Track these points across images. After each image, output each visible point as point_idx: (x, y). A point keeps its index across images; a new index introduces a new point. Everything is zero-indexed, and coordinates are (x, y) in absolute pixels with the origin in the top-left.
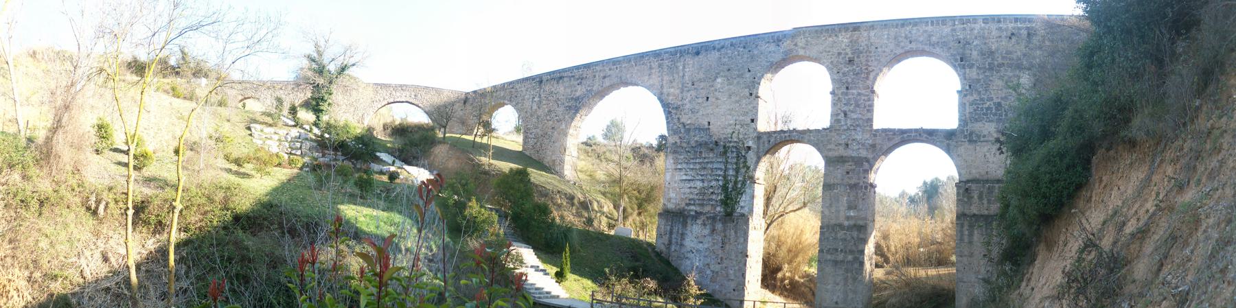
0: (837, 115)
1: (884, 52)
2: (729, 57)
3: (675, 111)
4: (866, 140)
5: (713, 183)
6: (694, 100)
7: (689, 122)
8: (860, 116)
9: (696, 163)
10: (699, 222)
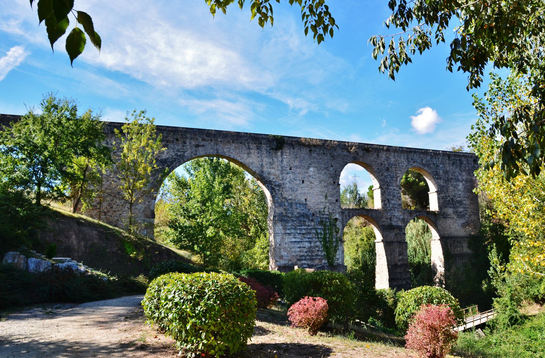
0: (385, 201)
1: (403, 166)
2: (317, 154)
3: (278, 188)
4: (400, 216)
5: (318, 244)
6: (293, 182)
7: (290, 198)
9: (302, 229)
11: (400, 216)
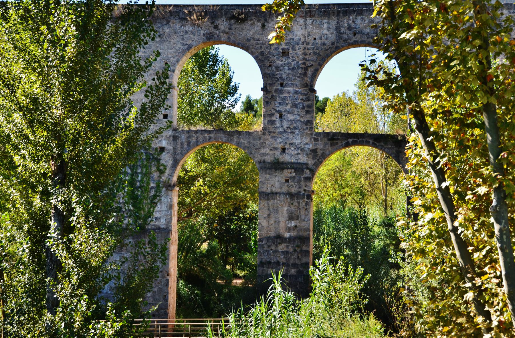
4: (307, 144)
8: (298, 118)
11: (307, 144)
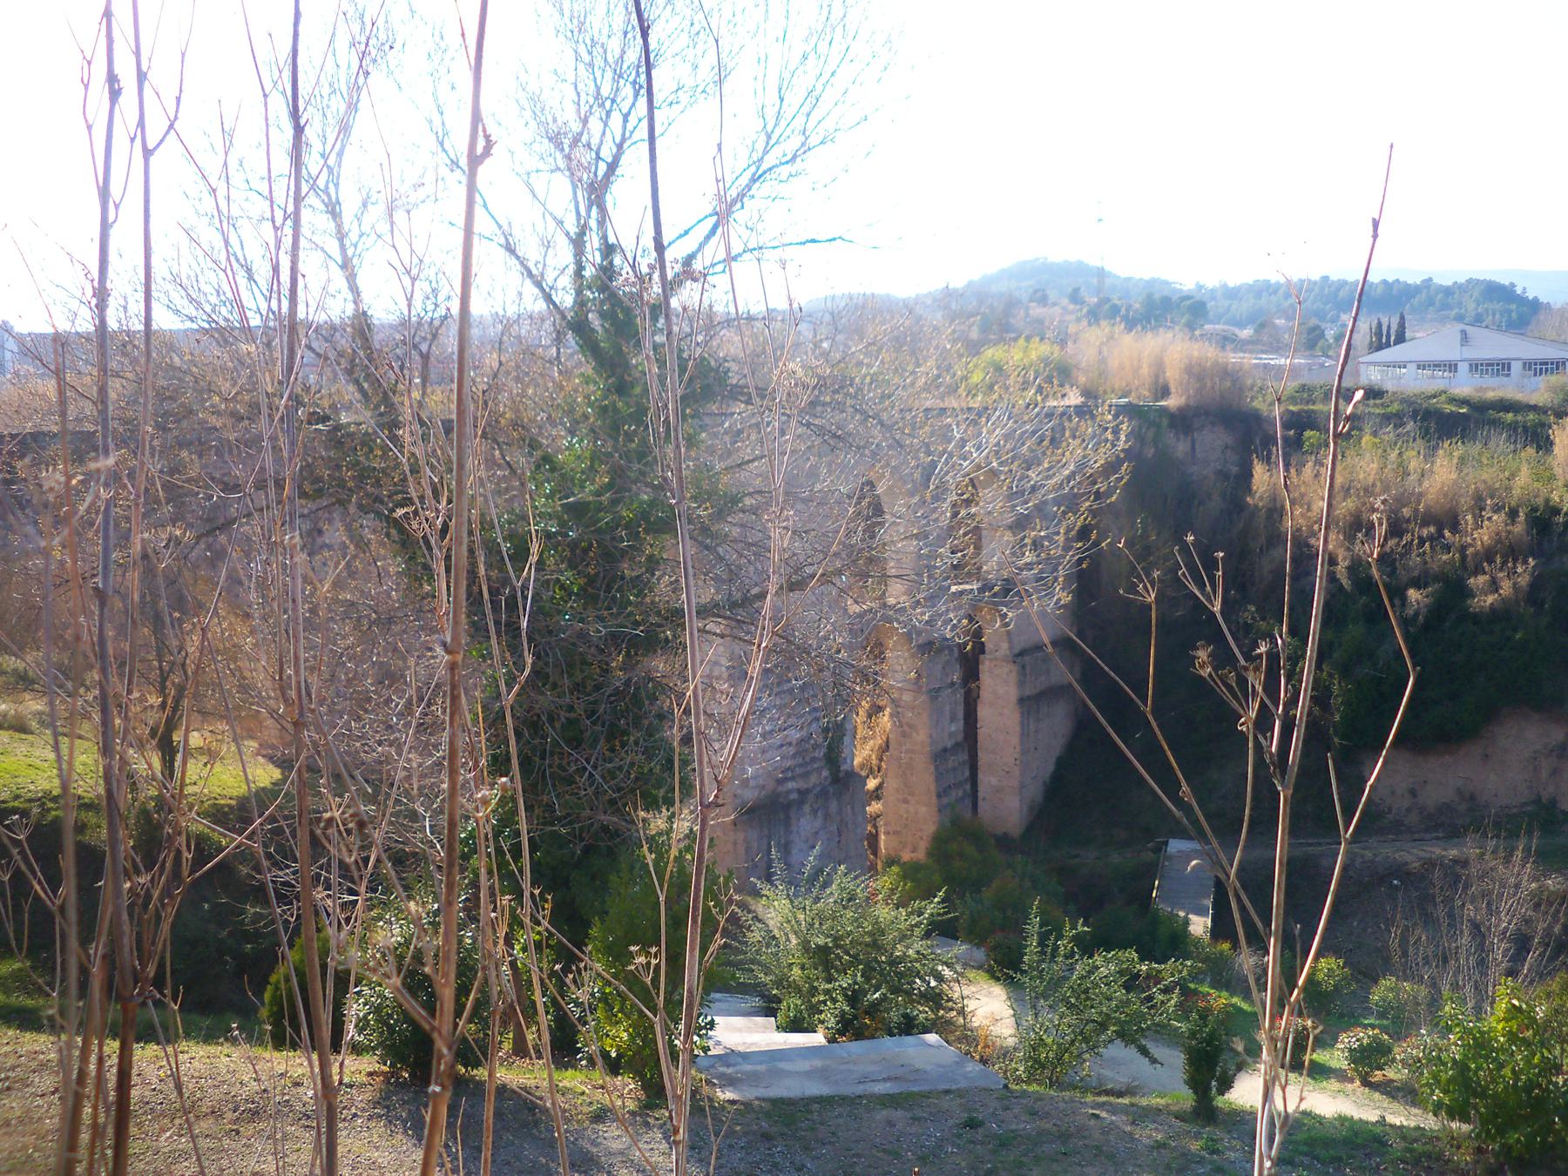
10: (807, 808)
